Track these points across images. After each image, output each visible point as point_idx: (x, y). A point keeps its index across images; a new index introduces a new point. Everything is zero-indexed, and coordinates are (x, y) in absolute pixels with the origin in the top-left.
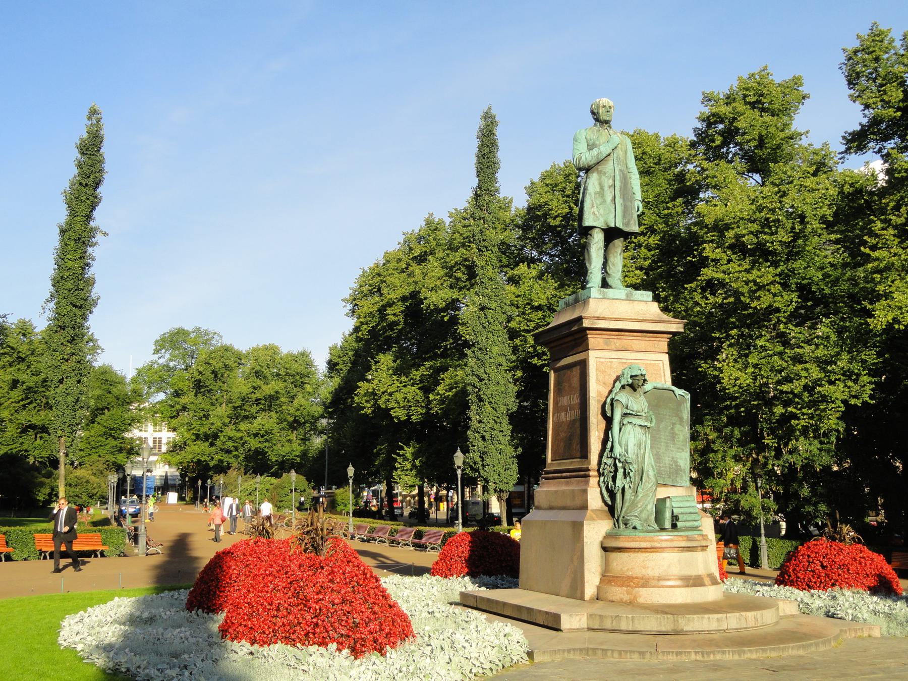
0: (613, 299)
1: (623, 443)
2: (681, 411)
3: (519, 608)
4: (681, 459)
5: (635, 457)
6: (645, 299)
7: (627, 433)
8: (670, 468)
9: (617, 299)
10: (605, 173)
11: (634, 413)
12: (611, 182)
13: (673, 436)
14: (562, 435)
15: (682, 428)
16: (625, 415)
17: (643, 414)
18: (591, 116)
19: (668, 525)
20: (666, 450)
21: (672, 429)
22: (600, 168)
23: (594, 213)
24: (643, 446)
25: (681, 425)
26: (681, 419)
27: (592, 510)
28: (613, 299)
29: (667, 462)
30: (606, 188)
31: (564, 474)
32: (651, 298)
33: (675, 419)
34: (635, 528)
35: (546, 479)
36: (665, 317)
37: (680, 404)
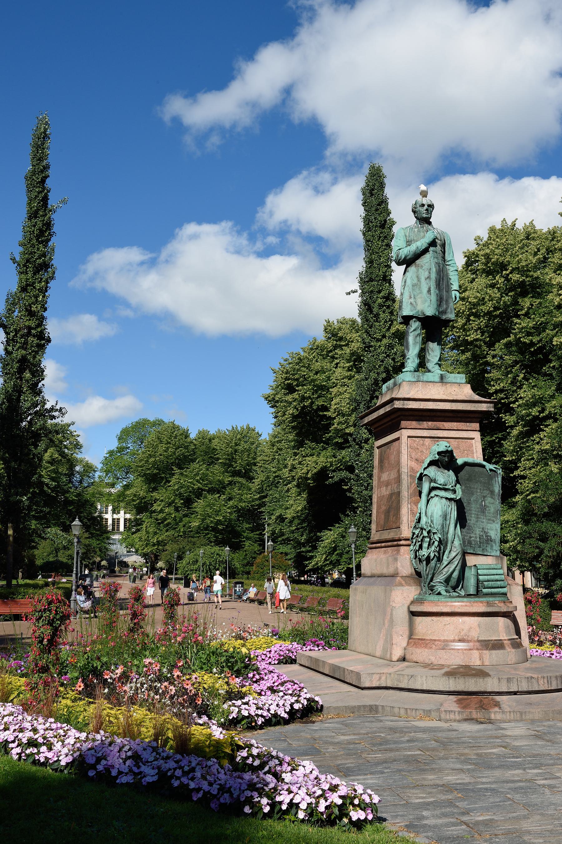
0: (427, 382)
1: (429, 514)
2: (492, 485)
3: (335, 668)
4: (492, 530)
6: (458, 382)
7: (433, 505)
8: (480, 537)
9: (431, 382)
10: (422, 266)
11: (441, 486)
12: (427, 274)
14: (383, 508)
15: (492, 501)
16: (432, 489)
18: (412, 214)
20: (477, 521)
22: (418, 262)
23: (411, 303)
24: (448, 517)
25: (492, 498)
26: (492, 492)
27: (402, 577)
28: (427, 382)
31: (383, 544)
32: (464, 381)
33: (486, 492)
34: (439, 594)
35: (371, 548)
36: (477, 398)
37: (491, 478)
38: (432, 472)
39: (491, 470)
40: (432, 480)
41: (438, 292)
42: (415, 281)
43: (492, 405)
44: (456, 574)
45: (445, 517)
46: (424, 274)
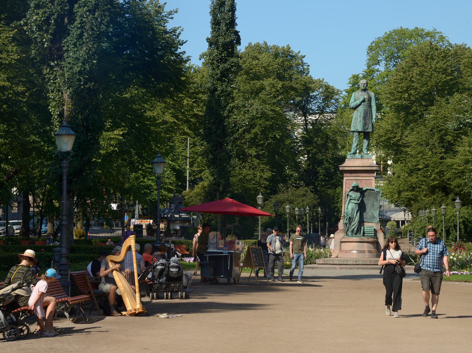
5: (350, 213)
13: (373, 205)
16: (350, 200)
17: (356, 199)
19: (362, 234)
21: (373, 203)
29: (370, 215)
30: (358, 116)
38: (351, 193)
39: (377, 192)
40: (351, 196)
41: (363, 121)
42: (356, 117)
43: (378, 167)
44: (356, 229)
45: (353, 209)
46: (359, 114)
